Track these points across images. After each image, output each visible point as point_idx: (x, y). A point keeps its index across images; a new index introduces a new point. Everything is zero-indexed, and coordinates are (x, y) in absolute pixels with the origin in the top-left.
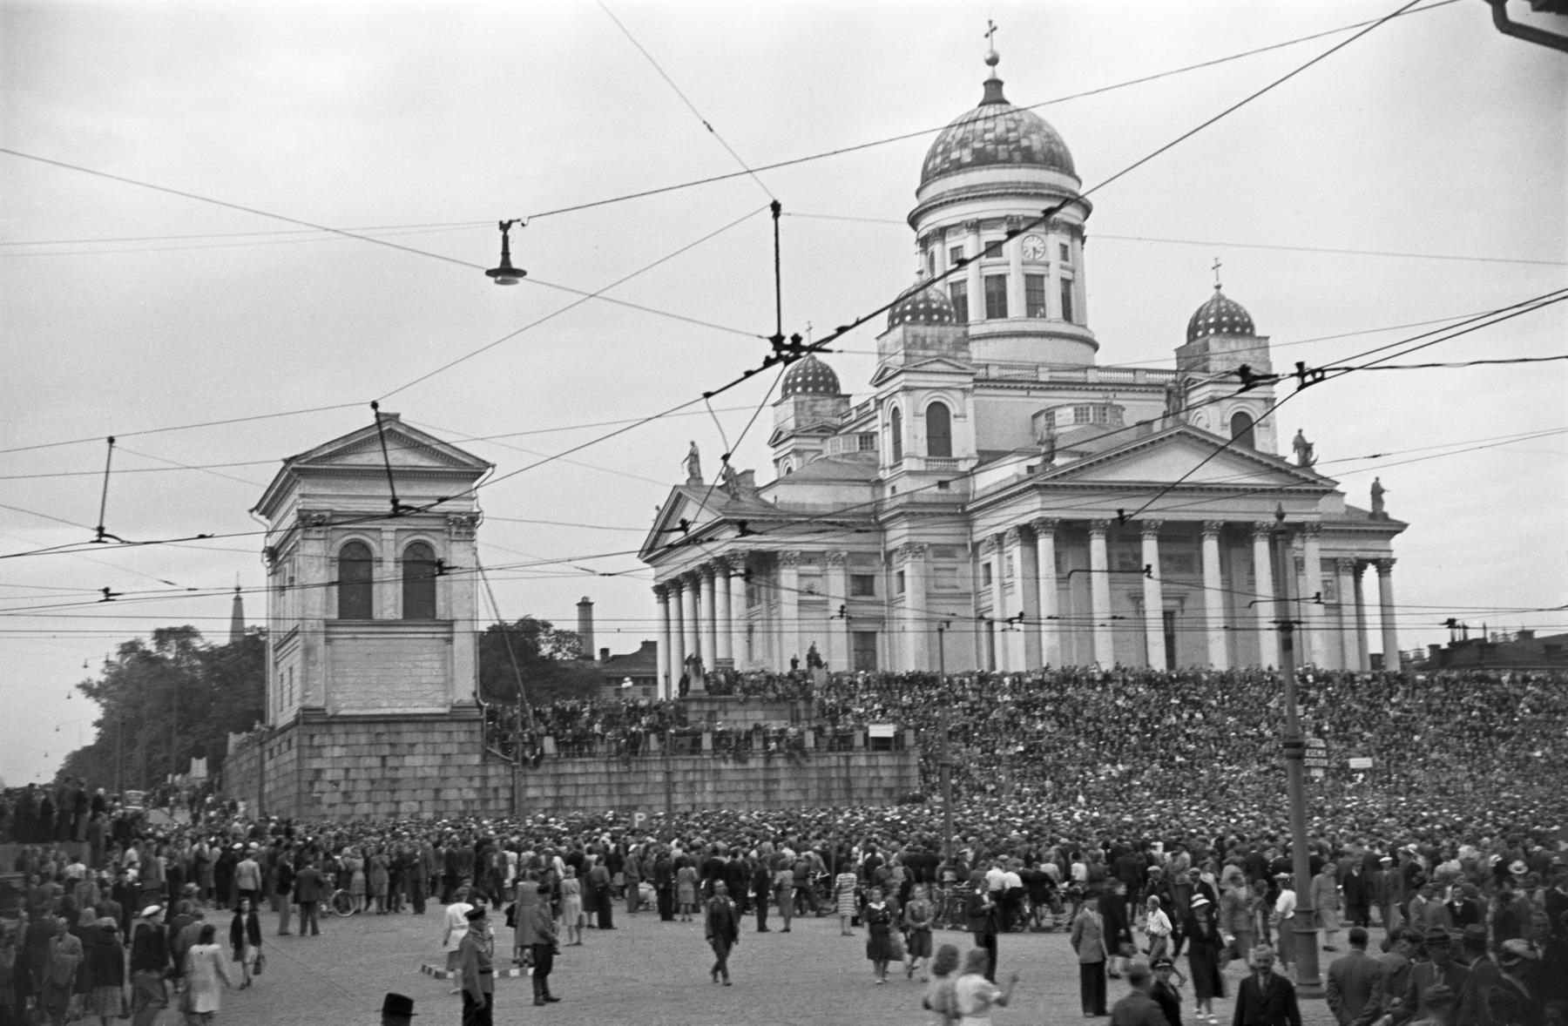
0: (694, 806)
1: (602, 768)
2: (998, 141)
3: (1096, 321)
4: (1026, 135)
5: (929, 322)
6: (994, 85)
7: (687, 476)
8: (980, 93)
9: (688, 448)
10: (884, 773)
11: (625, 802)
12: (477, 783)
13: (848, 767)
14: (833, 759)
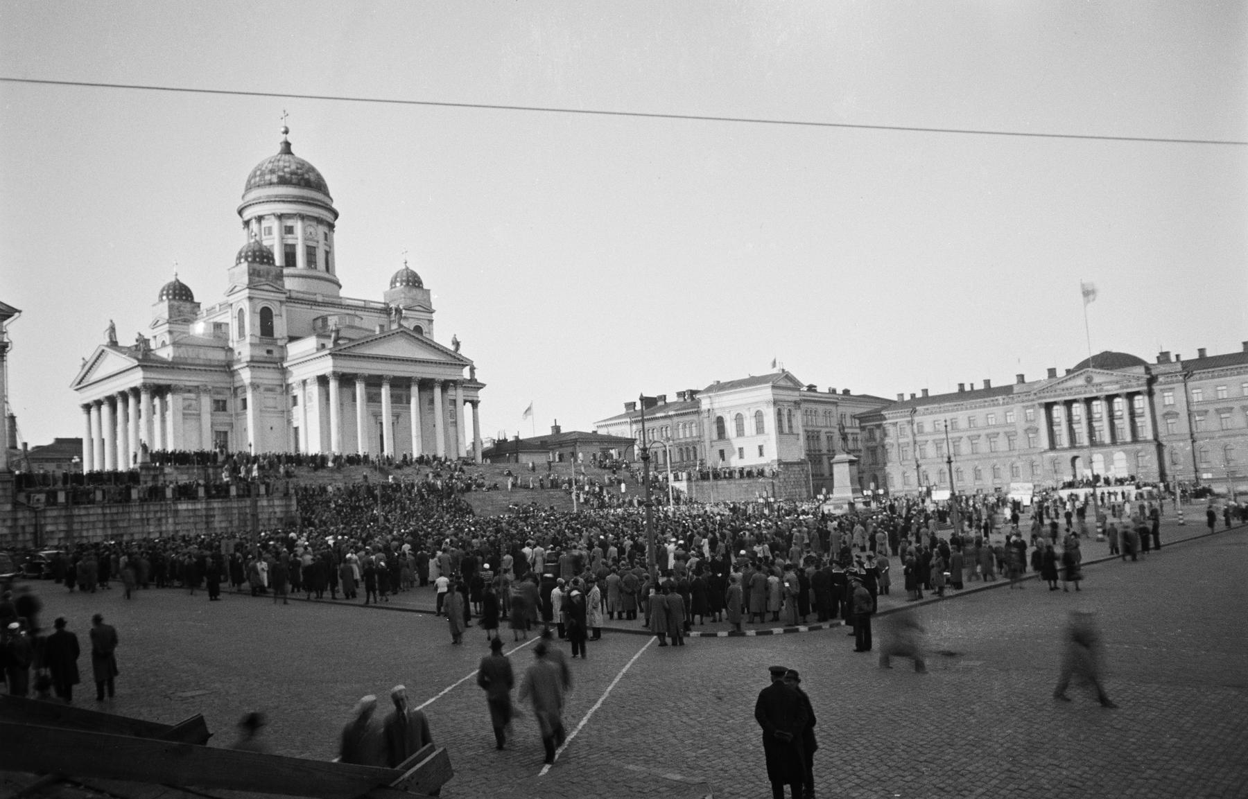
0: (161, 533)
1: (100, 511)
2: (292, 173)
3: (340, 272)
4: (307, 172)
5: (262, 263)
6: (287, 145)
7: (108, 340)
8: (279, 148)
9: (108, 325)
10: (277, 510)
11: (115, 532)
12: (9, 523)
14: (248, 502)
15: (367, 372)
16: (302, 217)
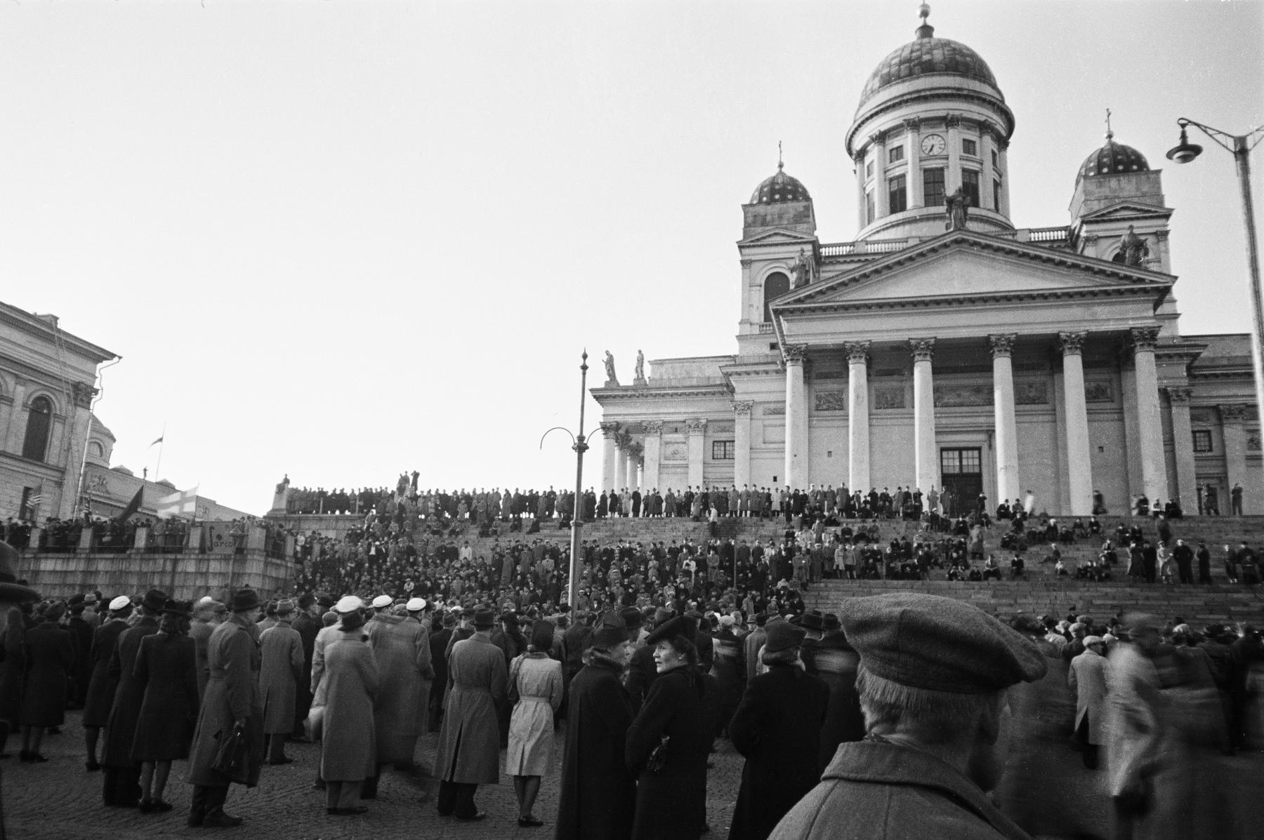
10: (214, 582)
13: (174, 572)
15: (864, 339)
16: (914, 125)
